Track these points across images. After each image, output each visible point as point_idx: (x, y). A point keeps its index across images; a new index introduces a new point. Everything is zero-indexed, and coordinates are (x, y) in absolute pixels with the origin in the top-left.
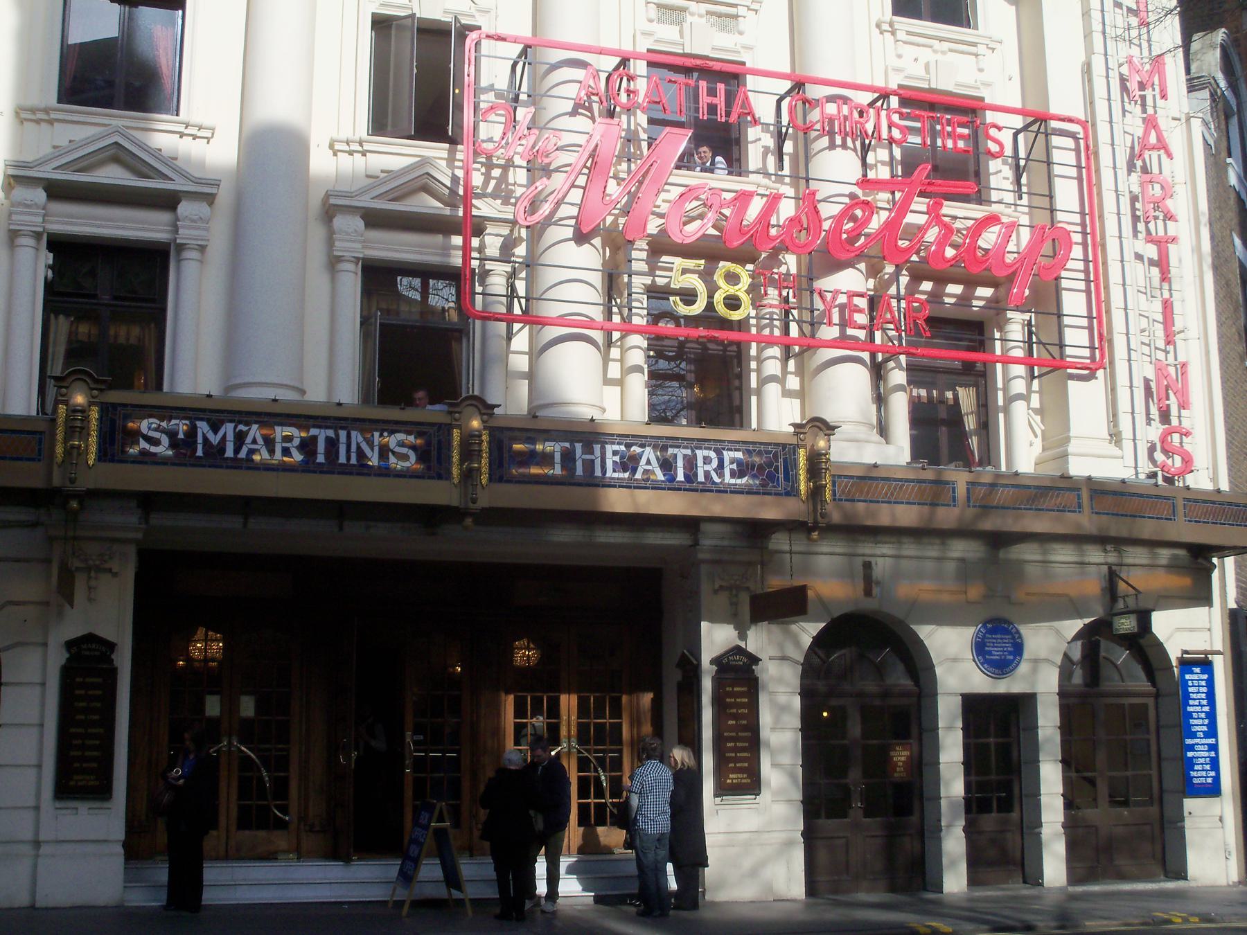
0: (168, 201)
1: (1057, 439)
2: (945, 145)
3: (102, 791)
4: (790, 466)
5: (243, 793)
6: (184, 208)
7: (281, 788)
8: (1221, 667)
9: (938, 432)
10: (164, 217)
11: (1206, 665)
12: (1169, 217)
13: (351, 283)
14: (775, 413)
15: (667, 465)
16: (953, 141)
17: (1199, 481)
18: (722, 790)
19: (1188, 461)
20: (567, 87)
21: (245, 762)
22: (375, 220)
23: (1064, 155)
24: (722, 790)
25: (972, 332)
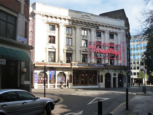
0: (72, 51)
1: (118, 63)
2: (112, 46)
3: (72, 82)
4: (106, 65)
5: (76, 82)
6: (73, 51)
7: (78, 82)
8: (126, 76)
9: (111, 63)
10: (72, 51)
11: (126, 76)
12: (125, 50)
13: (81, 55)
14: (103, 63)
15: (100, 66)
16: (113, 46)
17: (126, 66)
18: (101, 82)
19: (125, 65)
20: (92, 44)
21: (76, 81)
22: (83, 51)
23: (119, 47)
24: (101, 82)
25: (113, 57)
